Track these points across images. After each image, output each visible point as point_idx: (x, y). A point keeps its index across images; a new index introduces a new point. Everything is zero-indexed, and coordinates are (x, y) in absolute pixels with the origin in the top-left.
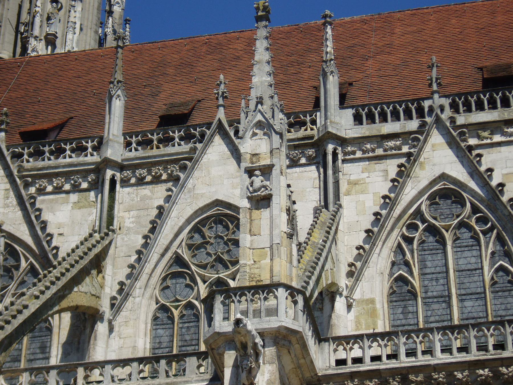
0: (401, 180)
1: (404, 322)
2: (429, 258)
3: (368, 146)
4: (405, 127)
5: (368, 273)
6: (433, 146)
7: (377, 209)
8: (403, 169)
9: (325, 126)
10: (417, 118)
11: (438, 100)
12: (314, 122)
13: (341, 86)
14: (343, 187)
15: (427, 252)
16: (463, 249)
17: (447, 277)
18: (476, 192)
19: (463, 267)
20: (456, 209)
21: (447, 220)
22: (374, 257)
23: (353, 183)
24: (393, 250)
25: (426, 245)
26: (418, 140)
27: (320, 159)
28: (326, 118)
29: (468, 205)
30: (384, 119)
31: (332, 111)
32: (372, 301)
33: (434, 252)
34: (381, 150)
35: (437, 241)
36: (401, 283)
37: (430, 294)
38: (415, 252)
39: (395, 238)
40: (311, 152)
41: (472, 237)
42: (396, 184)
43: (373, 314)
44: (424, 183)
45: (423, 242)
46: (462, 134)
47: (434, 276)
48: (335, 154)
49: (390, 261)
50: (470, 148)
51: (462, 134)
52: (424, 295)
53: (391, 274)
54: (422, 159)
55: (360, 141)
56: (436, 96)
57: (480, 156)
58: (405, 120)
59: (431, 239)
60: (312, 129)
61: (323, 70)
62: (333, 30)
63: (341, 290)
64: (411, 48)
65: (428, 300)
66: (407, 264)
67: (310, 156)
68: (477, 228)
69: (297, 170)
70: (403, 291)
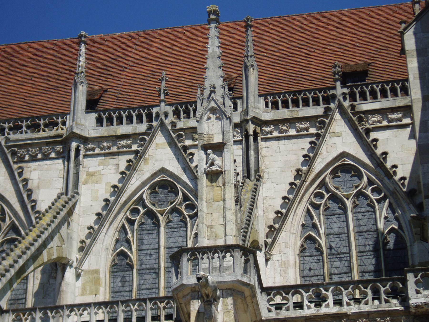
0: (128, 173)
1: (121, 289)
2: (146, 237)
3: (105, 144)
4: (136, 129)
5: (96, 248)
6: (157, 145)
7: (107, 196)
8: (131, 163)
9: (72, 127)
10: (147, 122)
11: (164, 108)
12: (64, 123)
13: (89, 93)
14: (83, 177)
15: (144, 232)
16: (173, 230)
17: (158, 253)
18: (187, 184)
19: (172, 245)
20: (171, 197)
21: (163, 206)
22: (101, 236)
23: (91, 175)
24: (118, 230)
25: (144, 226)
26: (144, 140)
27: (66, 154)
28: (73, 121)
29: (180, 194)
30: (120, 122)
31: (79, 115)
32: (97, 272)
33: (150, 232)
34: (116, 147)
35: (153, 223)
36: (122, 257)
37: (144, 267)
38: (135, 231)
39: (120, 220)
40: (59, 148)
41: (181, 221)
42: (124, 176)
43: (97, 282)
44: (147, 175)
45: (143, 224)
46: (180, 136)
47: (149, 251)
48: (78, 151)
49: (115, 238)
50: (185, 148)
51: (180, 136)
52: (139, 267)
53: (115, 249)
54: (147, 156)
55: (98, 140)
56: (163, 104)
57: (192, 154)
58: (137, 123)
59: (149, 221)
60: (62, 129)
61: (75, 81)
62: (86, 48)
63: (71, 262)
64: (161, 61)
65: (141, 271)
66: (128, 241)
67: (58, 151)
68: (185, 213)
69: (48, 162)
70: (123, 263)
